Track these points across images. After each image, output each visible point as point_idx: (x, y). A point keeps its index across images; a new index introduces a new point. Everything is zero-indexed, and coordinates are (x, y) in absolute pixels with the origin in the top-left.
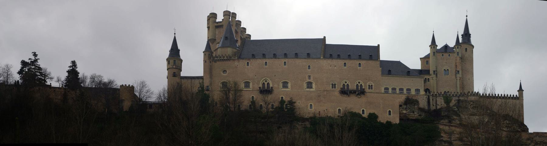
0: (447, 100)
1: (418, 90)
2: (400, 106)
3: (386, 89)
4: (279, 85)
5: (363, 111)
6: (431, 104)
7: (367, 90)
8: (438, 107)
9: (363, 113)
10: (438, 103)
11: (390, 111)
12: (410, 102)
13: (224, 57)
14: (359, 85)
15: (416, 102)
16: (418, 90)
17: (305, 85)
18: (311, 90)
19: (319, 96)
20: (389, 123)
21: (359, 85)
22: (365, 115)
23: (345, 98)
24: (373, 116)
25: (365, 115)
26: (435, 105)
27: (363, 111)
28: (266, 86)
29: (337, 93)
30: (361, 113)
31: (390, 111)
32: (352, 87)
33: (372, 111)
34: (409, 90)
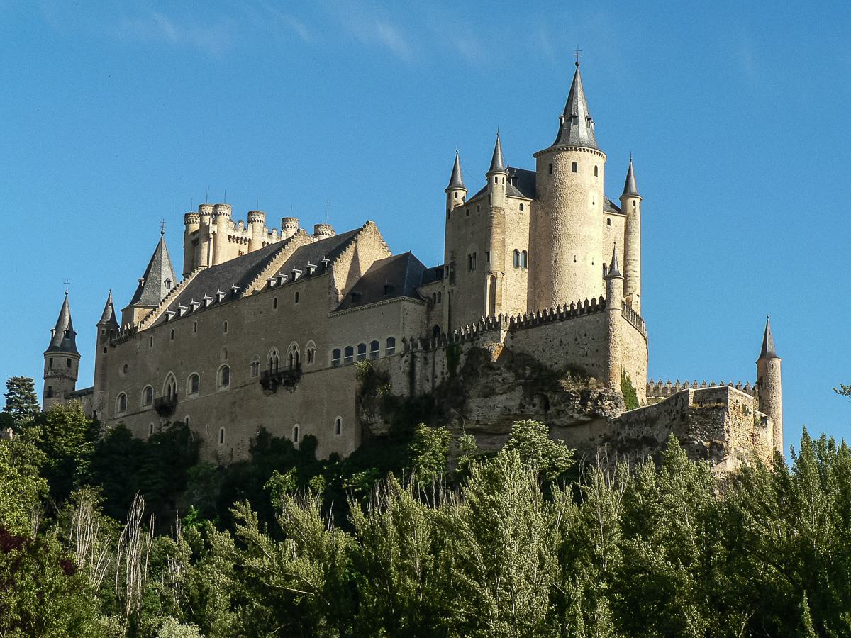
0: (453, 359)
1: (391, 342)
2: (358, 400)
3: (337, 353)
4: (185, 387)
5: (296, 428)
6: (418, 377)
7: (306, 366)
8: (438, 381)
9: (296, 440)
10: (438, 373)
11: (339, 421)
12: (372, 380)
13: (122, 334)
14: (294, 353)
15: (386, 379)
16: (391, 342)
17: (219, 376)
18: (228, 387)
19: (234, 403)
20: (334, 456)
21: (294, 353)
22: (296, 445)
23: (272, 399)
24: (310, 442)
25: (296, 445)
26: (430, 379)
27: (296, 428)
28: (171, 398)
29: (258, 389)
30: (293, 440)
31: (339, 421)
32: (285, 365)
33: (309, 429)
34: (375, 345)
